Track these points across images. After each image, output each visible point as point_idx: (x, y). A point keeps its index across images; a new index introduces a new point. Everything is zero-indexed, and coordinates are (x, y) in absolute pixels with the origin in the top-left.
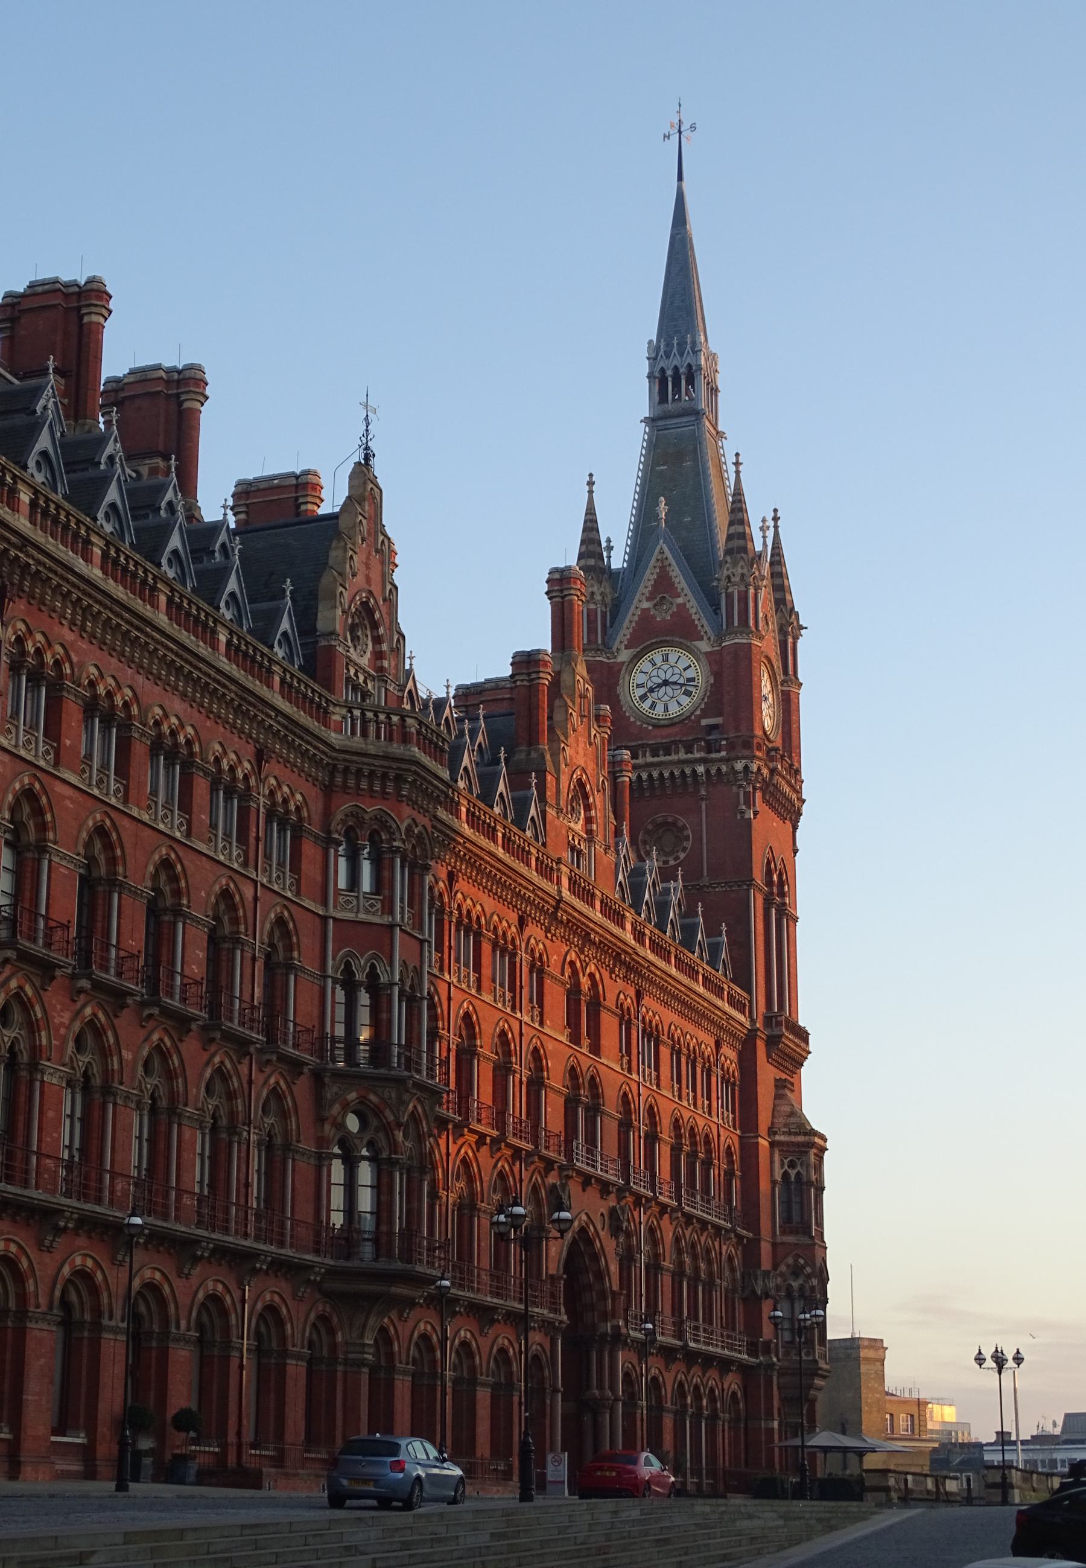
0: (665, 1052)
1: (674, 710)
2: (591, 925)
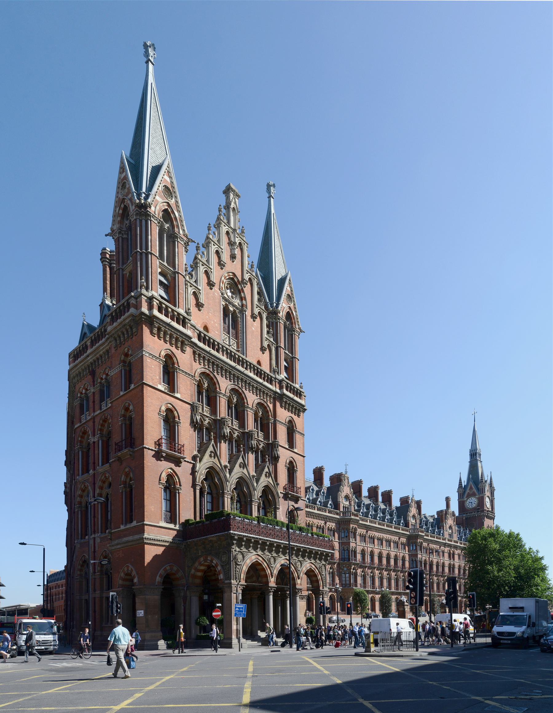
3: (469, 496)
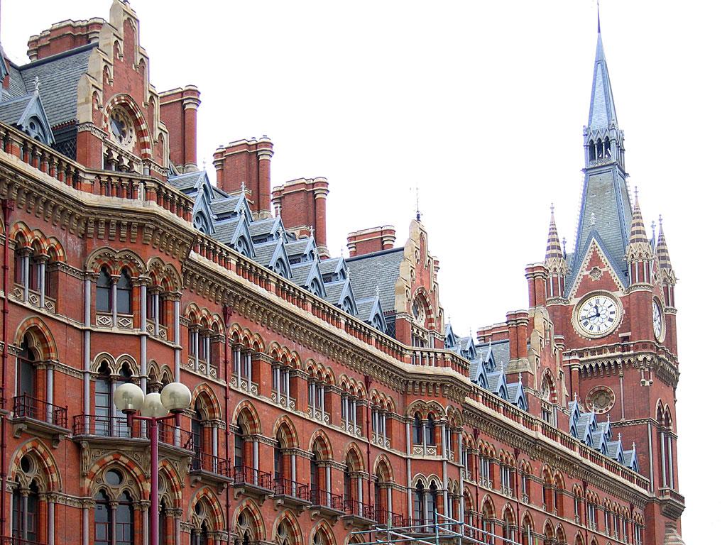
0: (601, 513)
1: (603, 329)
2: (556, 451)
3: (588, 291)
